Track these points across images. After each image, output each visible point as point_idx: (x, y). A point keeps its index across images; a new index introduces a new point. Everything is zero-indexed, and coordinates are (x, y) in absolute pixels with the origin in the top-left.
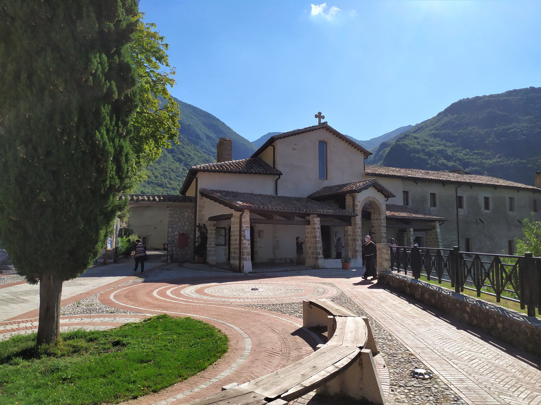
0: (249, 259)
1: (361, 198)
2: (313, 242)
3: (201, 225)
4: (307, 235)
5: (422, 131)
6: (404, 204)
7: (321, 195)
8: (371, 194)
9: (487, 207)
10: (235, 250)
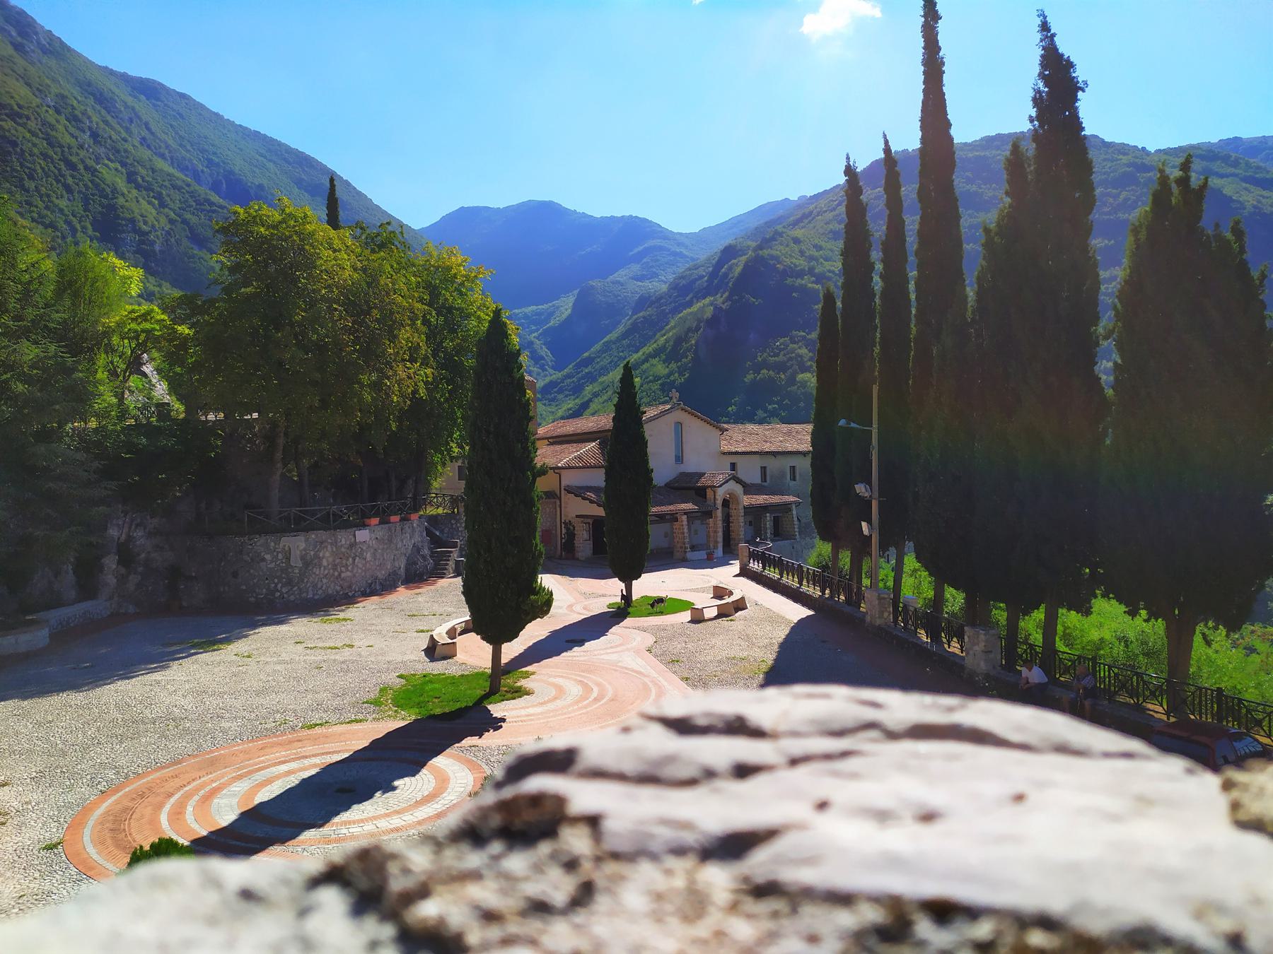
1: (721, 493)
3: (567, 521)
4: (674, 531)
5: (810, 222)
6: (762, 482)
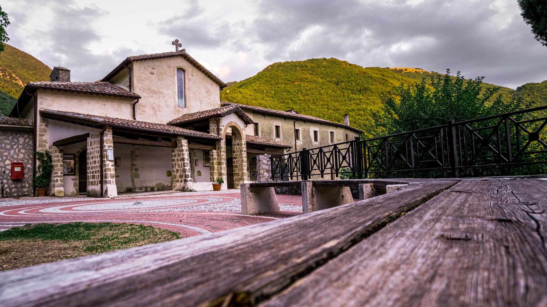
0: (113, 182)
2: (180, 165)
4: (173, 158)
7: (183, 121)
8: (233, 119)
9: (316, 139)
10: (94, 174)
